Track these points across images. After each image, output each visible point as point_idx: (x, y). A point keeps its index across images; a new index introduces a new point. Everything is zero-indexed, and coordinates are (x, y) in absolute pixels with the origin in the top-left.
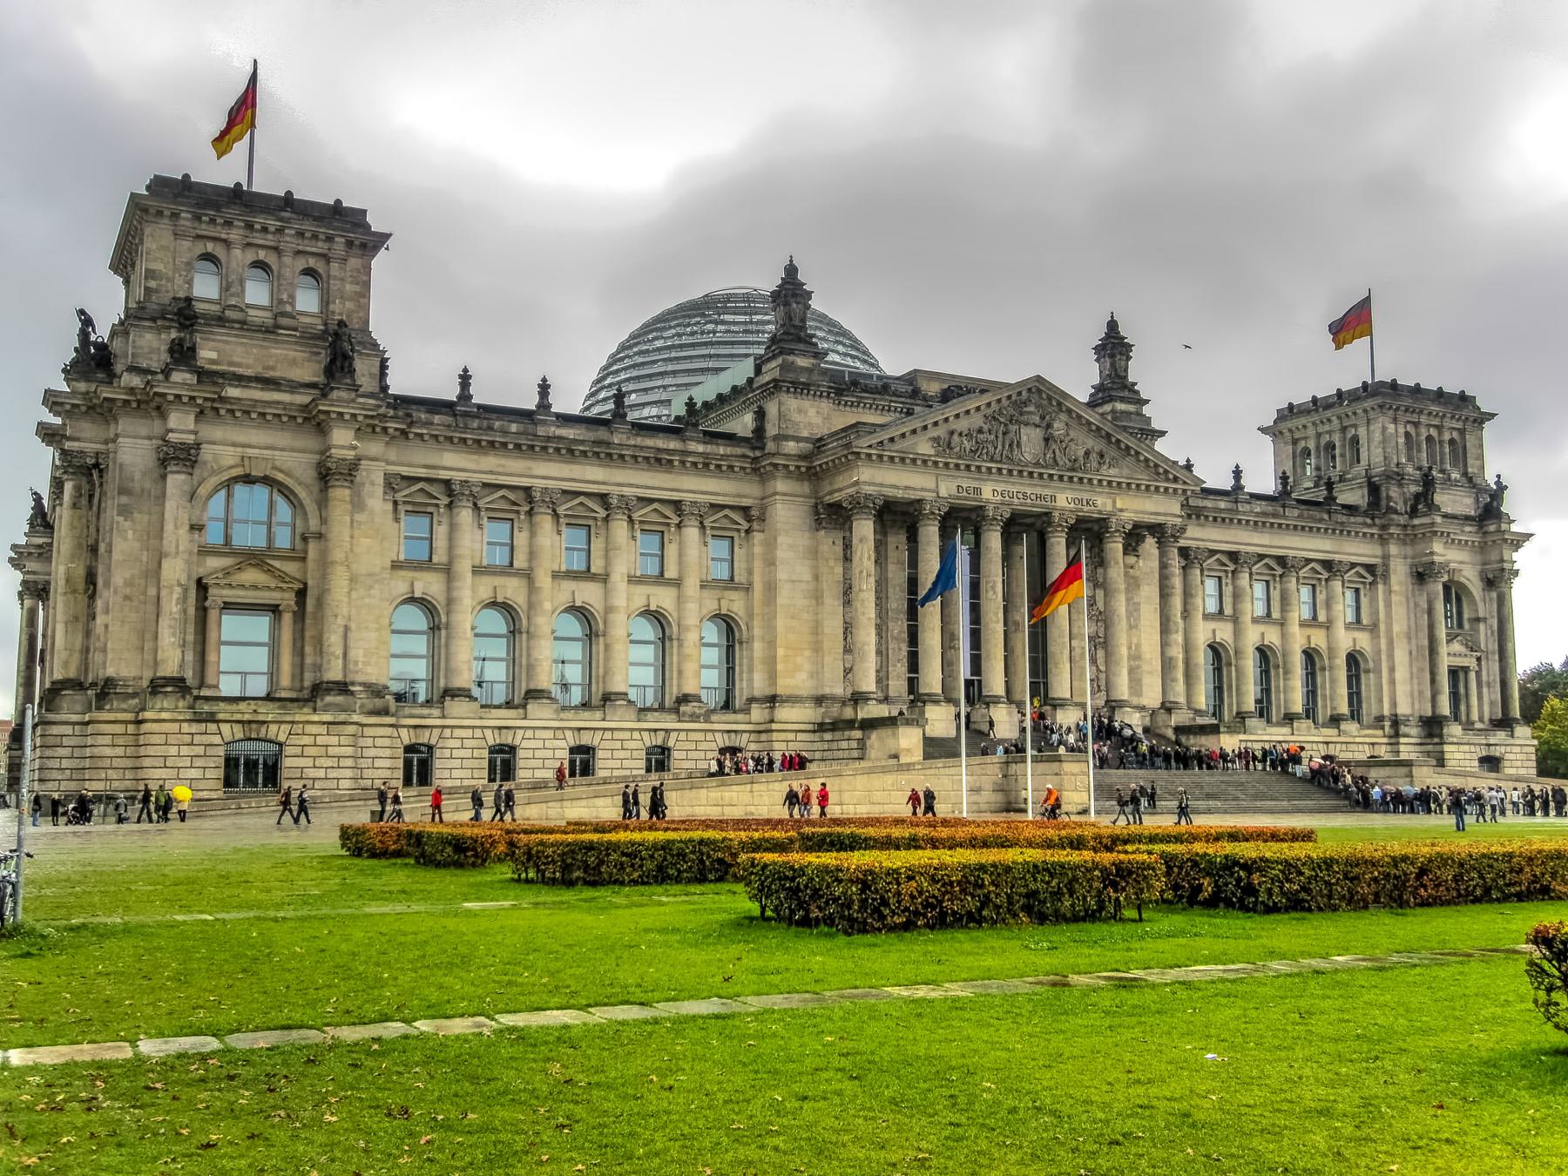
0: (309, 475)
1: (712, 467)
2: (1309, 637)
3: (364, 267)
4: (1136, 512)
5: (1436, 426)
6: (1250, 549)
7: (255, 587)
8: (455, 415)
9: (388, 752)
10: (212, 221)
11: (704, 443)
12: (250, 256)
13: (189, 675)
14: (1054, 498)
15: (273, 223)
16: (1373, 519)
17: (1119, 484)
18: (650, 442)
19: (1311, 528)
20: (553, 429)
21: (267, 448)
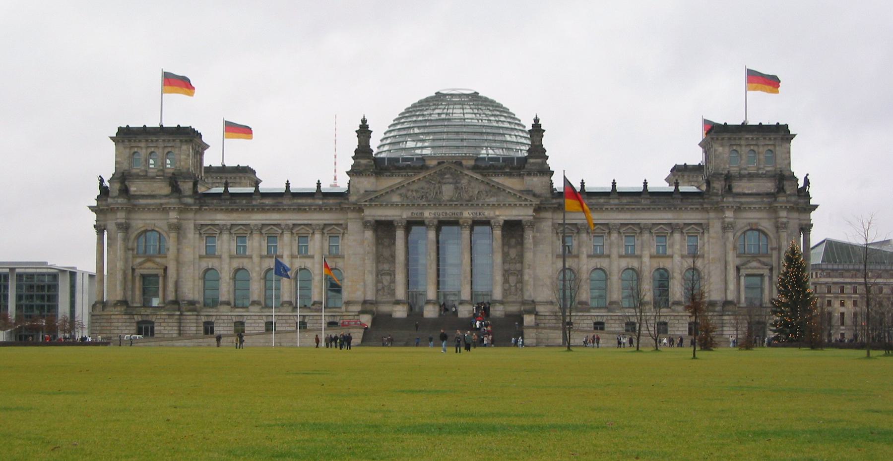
0: (166, 228)
1: (323, 209)
2: (659, 263)
3: (187, 148)
4: (506, 216)
5: (756, 145)
7: (149, 268)
8: (221, 200)
9: (195, 325)
10: (135, 141)
11: (322, 199)
12: (149, 150)
13: (129, 299)
15: (154, 139)
16: (704, 199)
17: (494, 205)
18: (300, 201)
20: (259, 201)
21: (152, 220)
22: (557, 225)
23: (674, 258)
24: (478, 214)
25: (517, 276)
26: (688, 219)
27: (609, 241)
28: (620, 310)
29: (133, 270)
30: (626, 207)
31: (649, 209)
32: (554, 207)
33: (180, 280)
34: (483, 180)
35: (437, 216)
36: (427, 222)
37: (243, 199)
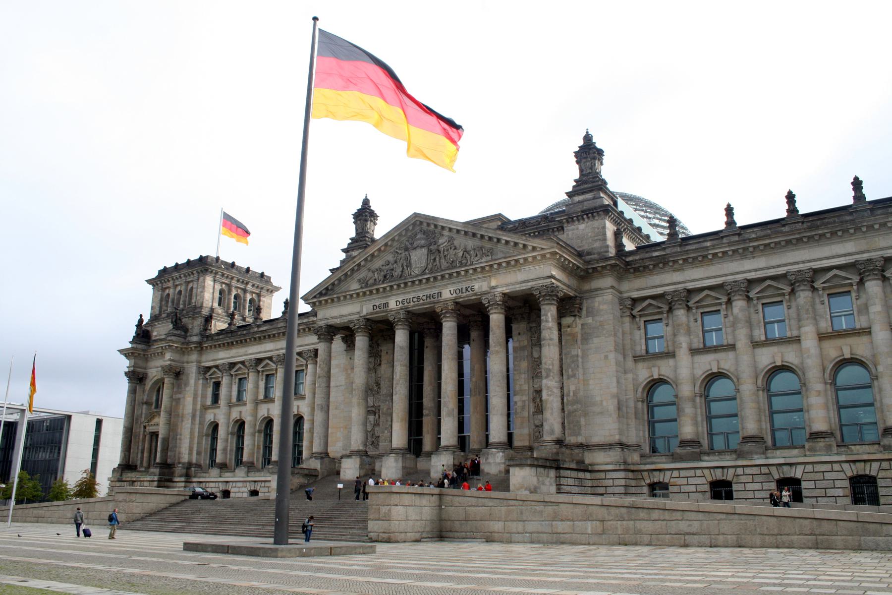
4: (507, 285)
10: (165, 282)
13: (138, 463)
14: (440, 294)
17: (483, 268)
19: (812, 237)
20: (256, 329)
22: (630, 302)
23: (873, 334)
24: (464, 290)
27: (731, 318)
28: (763, 453)
29: (145, 427)
30: (751, 245)
31: (799, 240)
32: (613, 266)
33: (178, 437)
34: (466, 230)
35: (406, 304)
36: (391, 319)
37: (243, 330)
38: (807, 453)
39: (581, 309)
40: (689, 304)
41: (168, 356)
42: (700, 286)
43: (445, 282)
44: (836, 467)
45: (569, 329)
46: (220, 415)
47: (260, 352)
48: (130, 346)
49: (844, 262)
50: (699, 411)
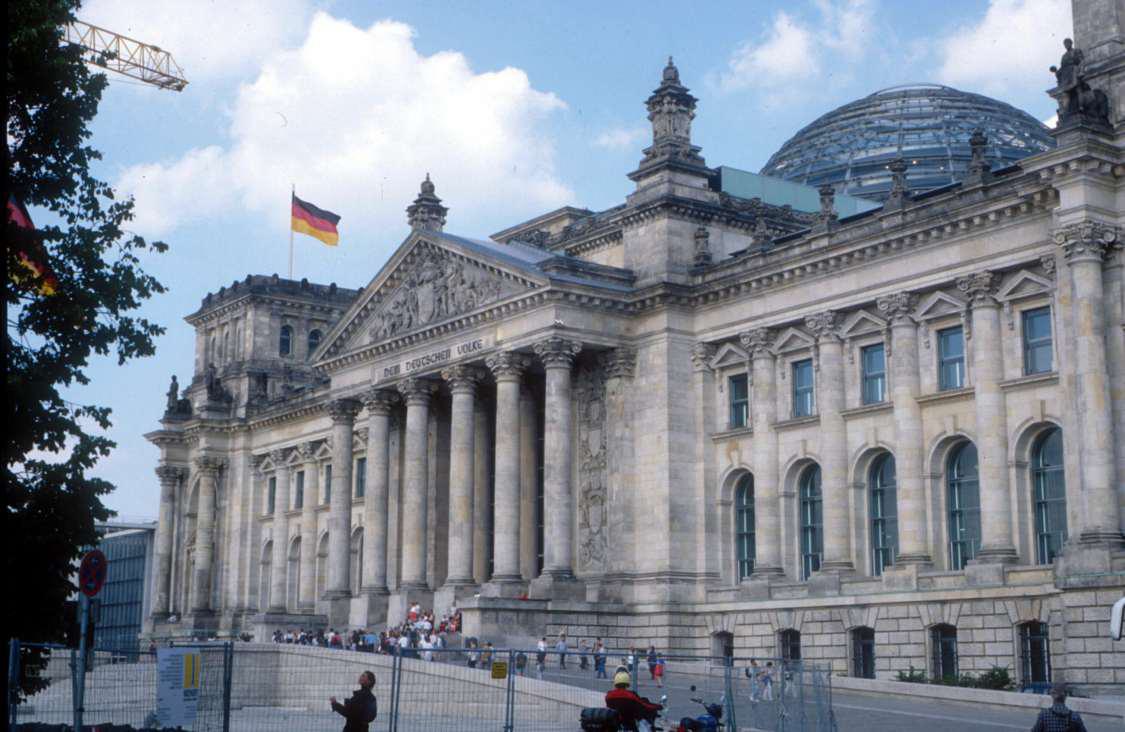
4: (512, 339)
6: (824, 307)
14: (448, 352)
24: (472, 347)
25: (602, 504)
26: (1001, 254)
30: (831, 255)
33: (225, 567)
37: (297, 398)
38: (885, 589)
39: (634, 365)
40: (771, 350)
41: (203, 442)
42: (781, 322)
43: (452, 335)
44: (912, 609)
45: (613, 398)
46: (273, 531)
47: (315, 432)
48: (161, 427)
49: (946, 280)
50: (783, 519)
